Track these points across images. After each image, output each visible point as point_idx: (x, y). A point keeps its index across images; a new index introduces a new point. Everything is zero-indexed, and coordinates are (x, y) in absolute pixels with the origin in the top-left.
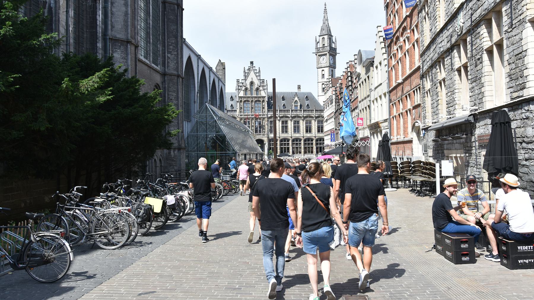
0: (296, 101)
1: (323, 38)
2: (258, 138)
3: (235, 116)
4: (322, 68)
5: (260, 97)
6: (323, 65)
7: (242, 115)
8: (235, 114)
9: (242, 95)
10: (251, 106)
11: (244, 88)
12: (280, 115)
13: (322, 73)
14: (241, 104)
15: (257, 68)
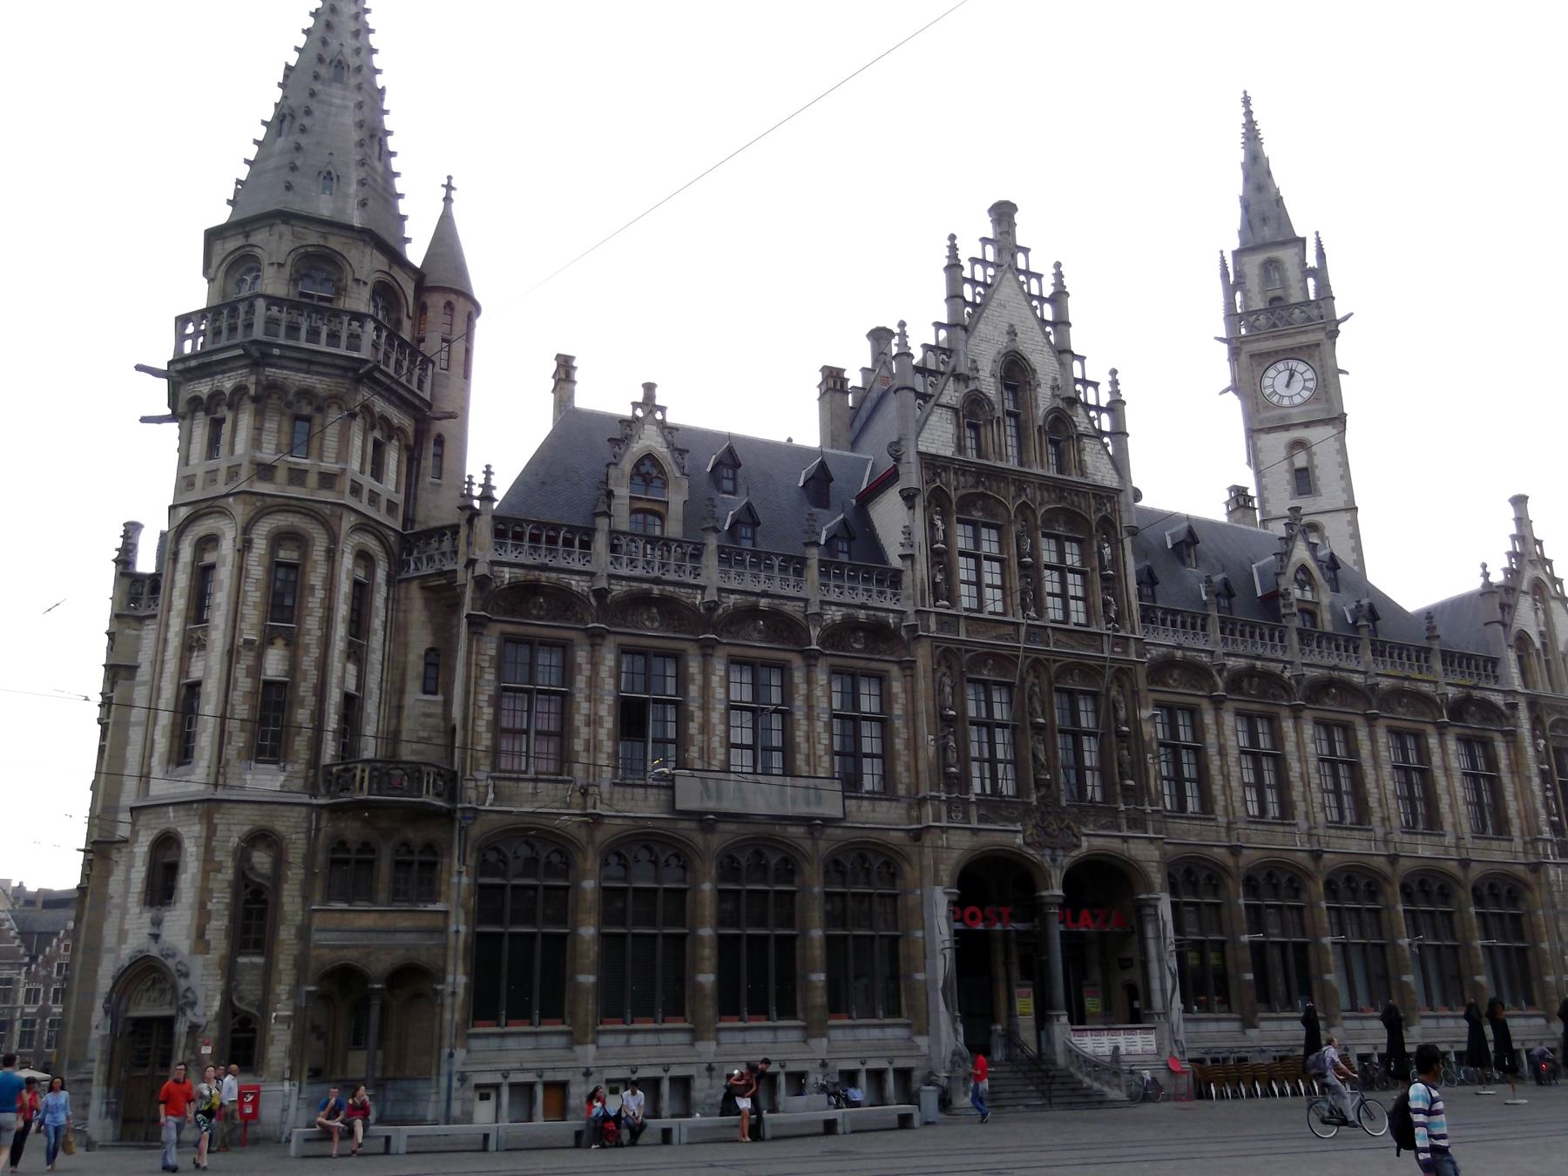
0: (1303, 568)
1: (1271, 266)
2: (1098, 842)
3: (891, 619)
4: (1287, 428)
5: (1080, 490)
6: (1294, 411)
7: (947, 621)
8: (888, 604)
9: (949, 452)
10: (1020, 555)
11: (952, 394)
12: (1231, 663)
13: (1292, 464)
14: (939, 523)
15: (1040, 262)
